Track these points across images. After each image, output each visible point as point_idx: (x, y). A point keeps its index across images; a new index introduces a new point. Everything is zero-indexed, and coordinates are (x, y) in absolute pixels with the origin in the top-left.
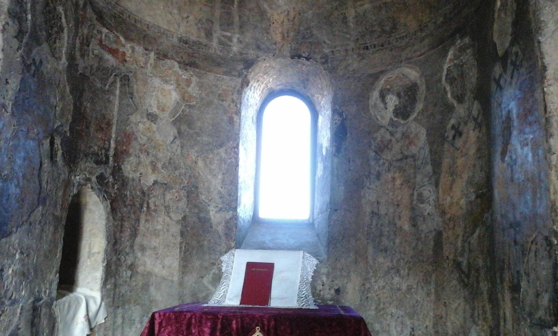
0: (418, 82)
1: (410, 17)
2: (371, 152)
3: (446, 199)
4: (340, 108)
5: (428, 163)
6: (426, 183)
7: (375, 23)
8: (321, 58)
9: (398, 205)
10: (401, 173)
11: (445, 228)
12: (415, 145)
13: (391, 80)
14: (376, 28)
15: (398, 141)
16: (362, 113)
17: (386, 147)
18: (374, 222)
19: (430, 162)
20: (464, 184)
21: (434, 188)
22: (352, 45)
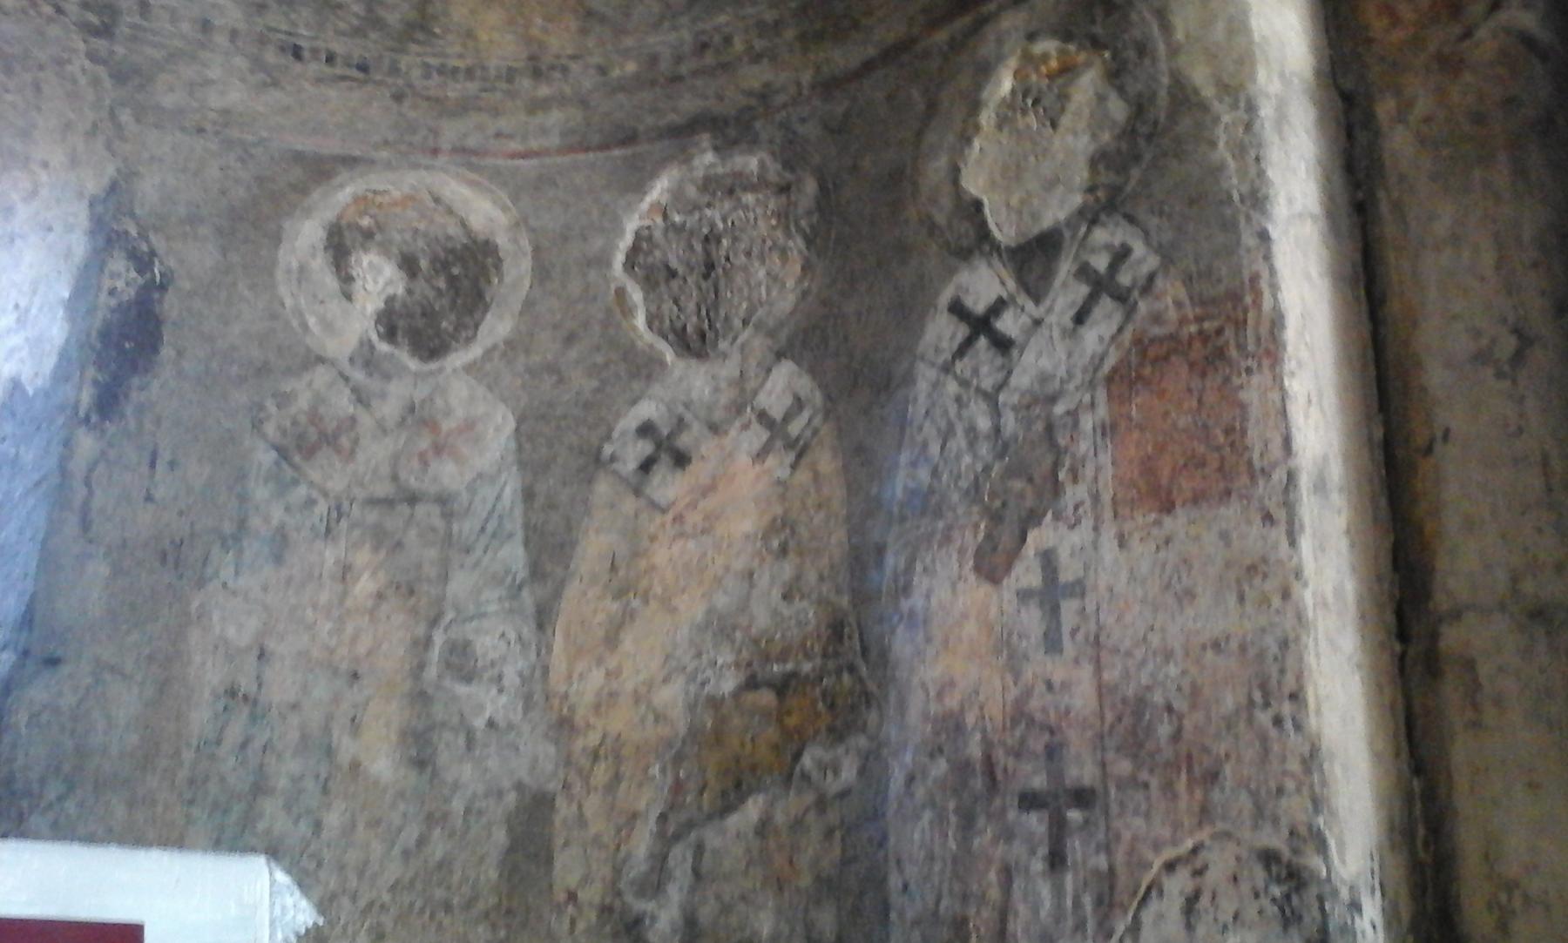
0: (502, 240)
2: (261, 445)
4: (143, 235)
5: (511, 536)
9: (355, 676)
10: (382, 554)
11: (566, 786)
12: (459, 459)
13: (379, 199)
15: (382, 429)
17: (329, 439)
18: (234, 733)
19: (520, 535)
20: (684, 633)
21: (528, 631)
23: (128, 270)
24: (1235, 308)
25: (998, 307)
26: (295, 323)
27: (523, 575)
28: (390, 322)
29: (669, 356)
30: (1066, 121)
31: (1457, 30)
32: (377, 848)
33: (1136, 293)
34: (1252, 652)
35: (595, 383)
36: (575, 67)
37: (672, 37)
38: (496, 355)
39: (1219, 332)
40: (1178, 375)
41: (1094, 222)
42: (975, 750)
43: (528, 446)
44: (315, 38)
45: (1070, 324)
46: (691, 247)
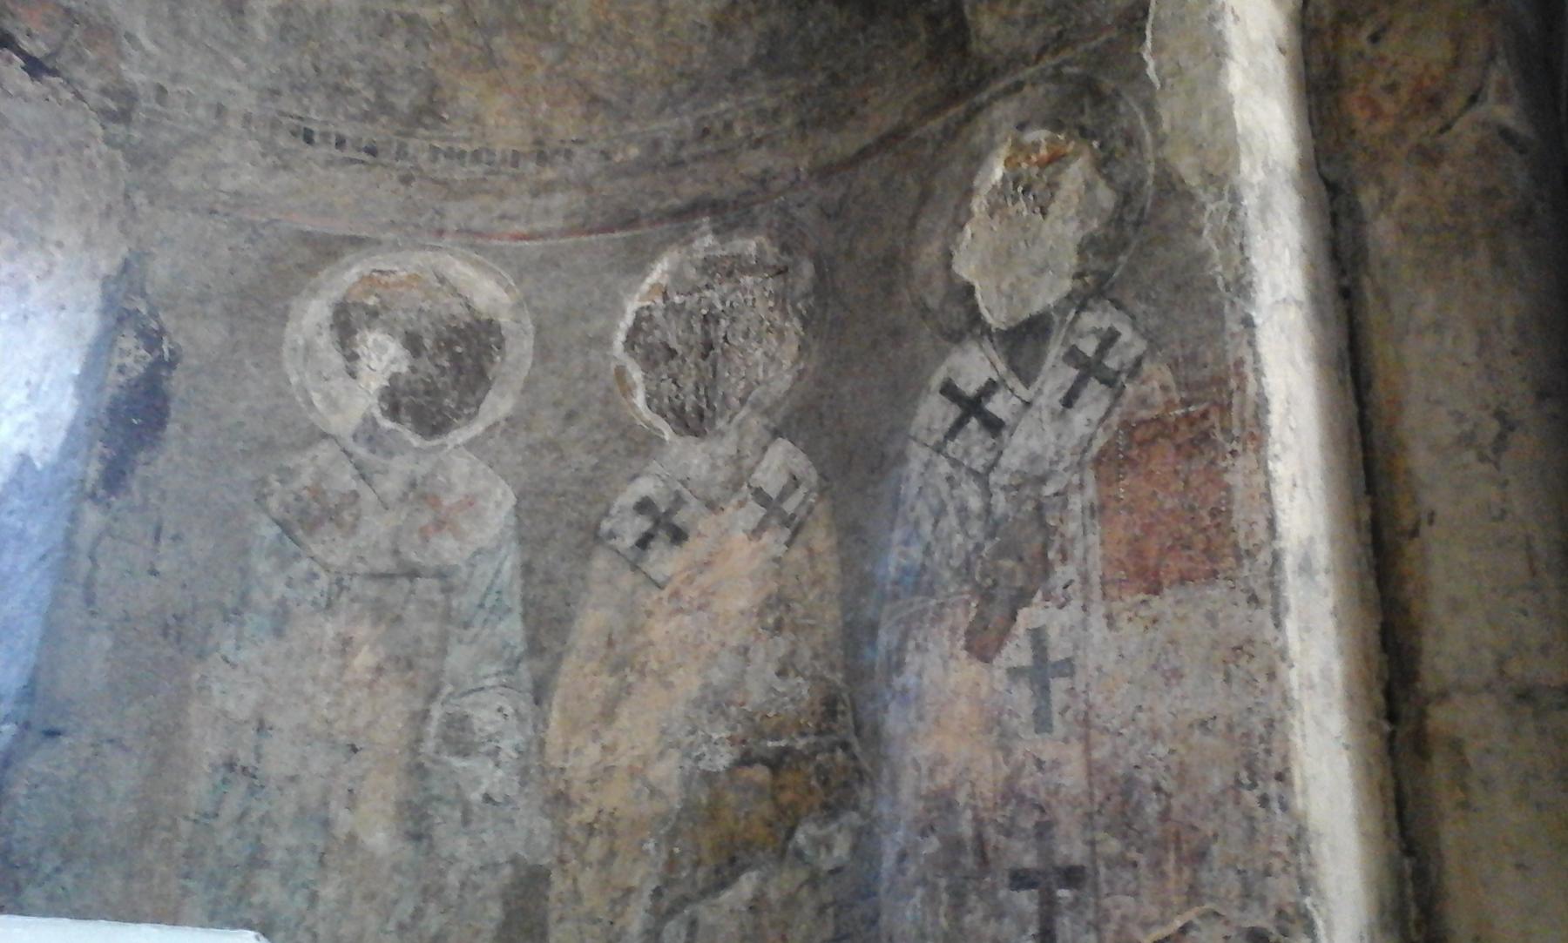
0: (504, 320)
1: (501, 101)
2: (265, 519)
3: (578, 751)
5: (509, 610)
7: (356, 65)
8: (104, 91)
9: (354, 750)
10: (383, 627)
11: (562, 861)
12: (458, 534)
13: (385, 279)
14: (356, 83)
16: (248, 362)
17: (332, 515)
18: (231, 808)
19: (518, 609)
21: (525, 706)
22: (247, 100)
23: (137, 348)
24: (1220, 391)
25: (990, 388)
26: (299, 399)
27: (520, 649)
28: (394, 400)
29: (668, 434)
30: (1055, 208)
31: (1436, 123)
32: (372, 921)
33: (1123, 377)
34: (1238, 732)
35: (594, 461)
36: (579, 151)
37: (675, 122)
38: (498, 431)
39: (1204, 415)
40: (1163, 459)
41: (1082, 307)
42: (966, 829)
43: (527, 522)
44: (326, 123)
45: (1060, 407)
46: (691, 328)
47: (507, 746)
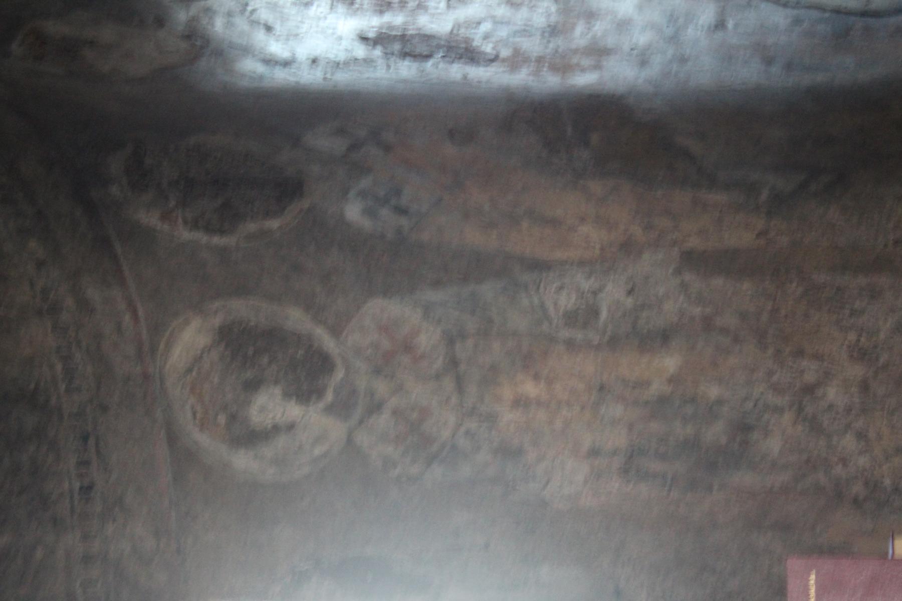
0: (217, 321)
6: (536, 301)
11: (674, 243)
15: (399, 389)
18: (656, 466)
47: (586, 285)
